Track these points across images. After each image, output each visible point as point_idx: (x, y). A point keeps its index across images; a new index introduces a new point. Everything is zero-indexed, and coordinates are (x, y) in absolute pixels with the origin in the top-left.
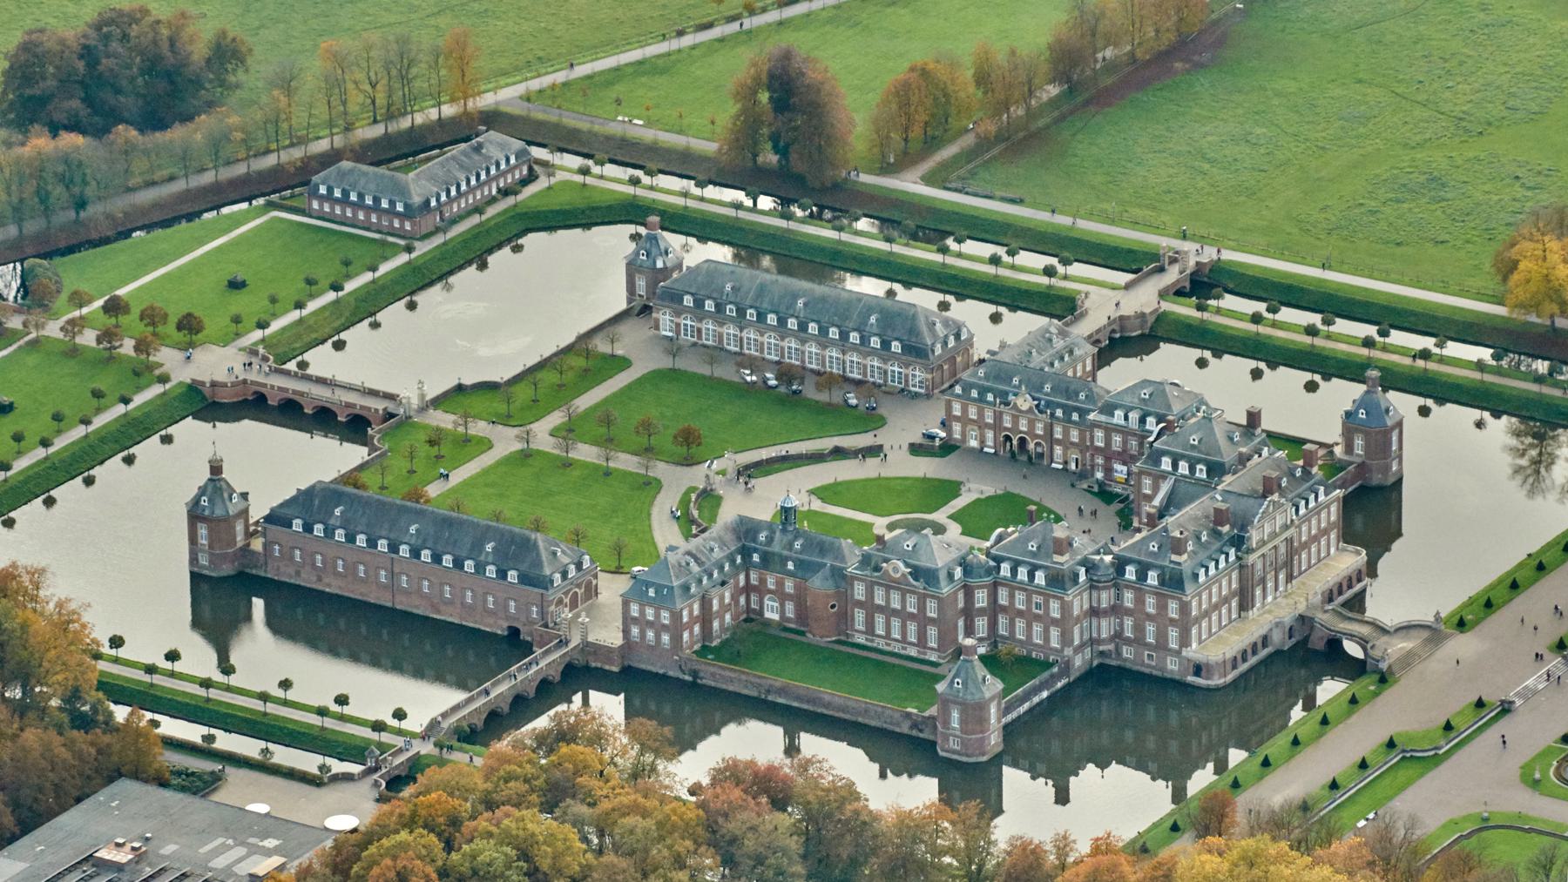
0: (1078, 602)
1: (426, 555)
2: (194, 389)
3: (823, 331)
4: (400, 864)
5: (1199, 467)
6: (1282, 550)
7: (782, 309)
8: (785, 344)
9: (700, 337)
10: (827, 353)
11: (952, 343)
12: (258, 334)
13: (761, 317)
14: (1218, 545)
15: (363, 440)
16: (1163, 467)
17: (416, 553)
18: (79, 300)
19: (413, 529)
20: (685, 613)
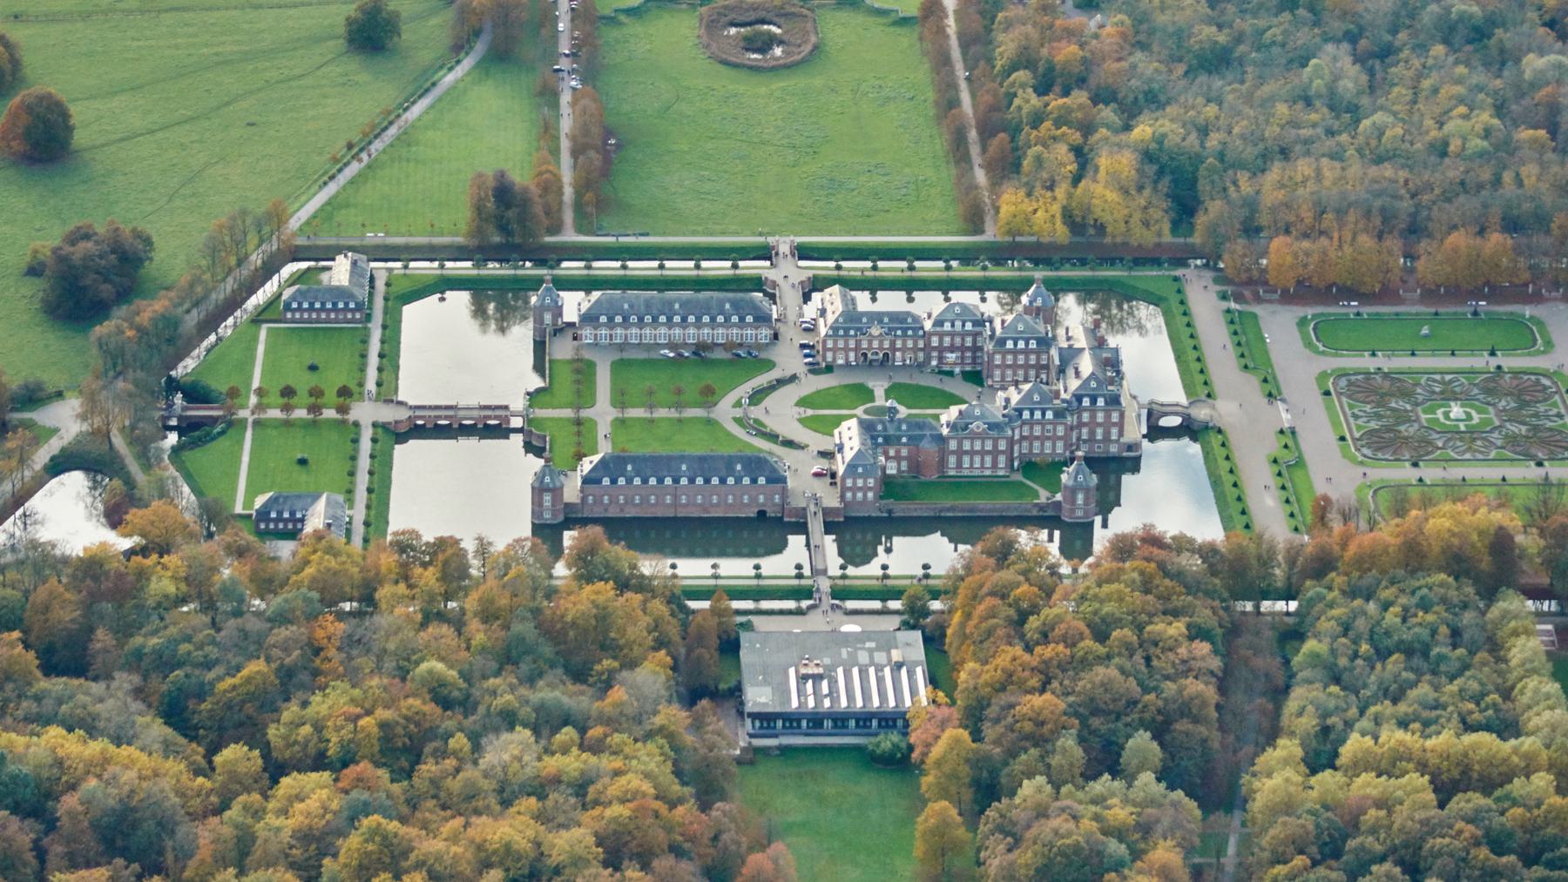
1: (700, 481)
3: (699, 319)
13: (655, 319)
17: (692, 481)
19: (684, 467)
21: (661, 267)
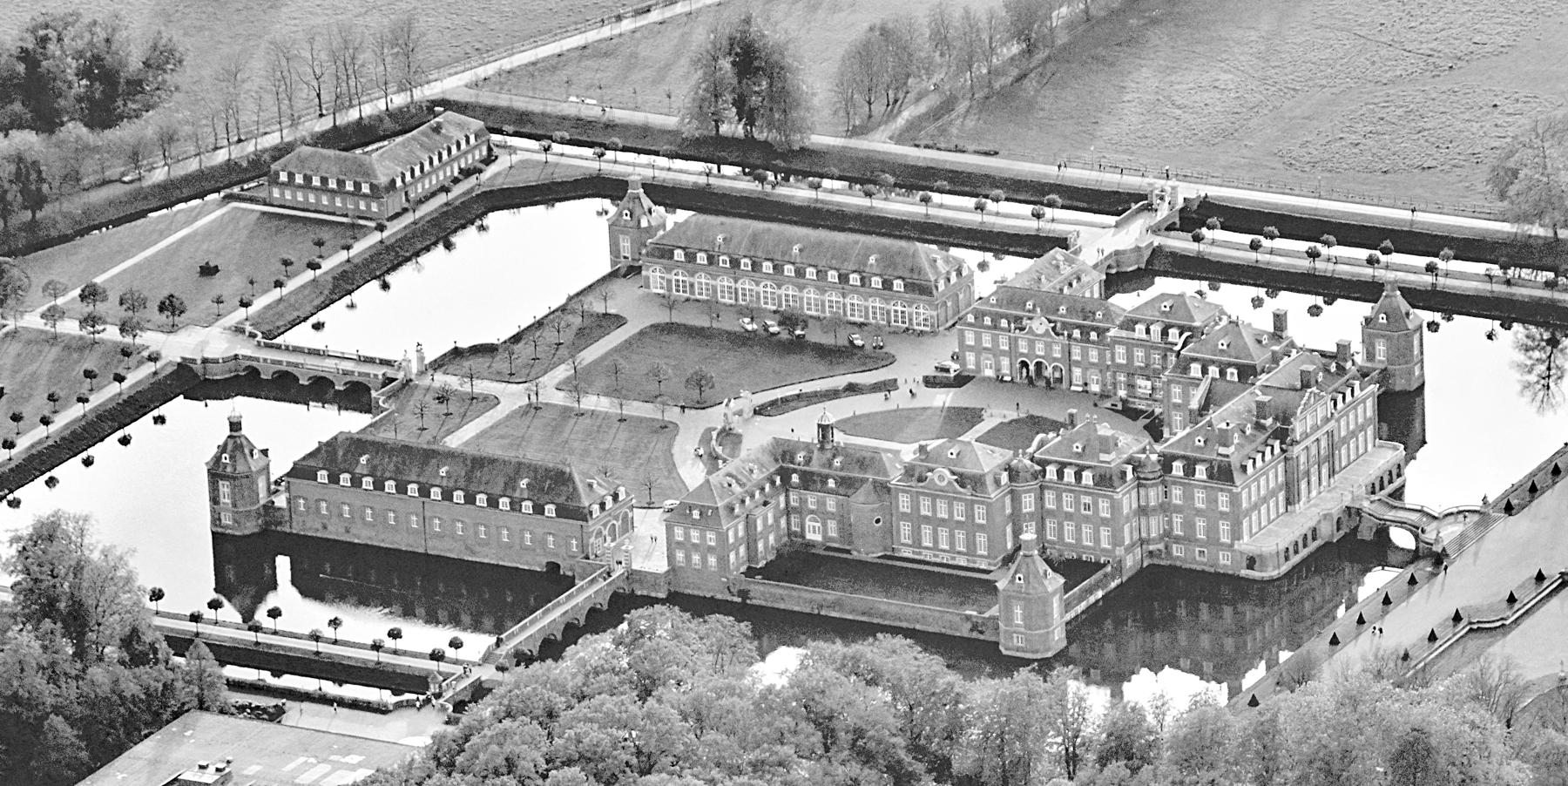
0: (1127, 498)
1: (459, 496)
2: (184, 367)
4: (508, 748)
5: (1229, 370)
6: (1323, 444)
7: (778, 256)
8: (782, 292)
9: (692, 293)
10: (826, 297)
11: (954, 278)
12: (242, 313)
13: (756, 266)
14: (1264, 437)
15: (366, 408)
16: (1192, 374)
18: (53, 289)
20: (731, 533)
21: (1255, 246)
